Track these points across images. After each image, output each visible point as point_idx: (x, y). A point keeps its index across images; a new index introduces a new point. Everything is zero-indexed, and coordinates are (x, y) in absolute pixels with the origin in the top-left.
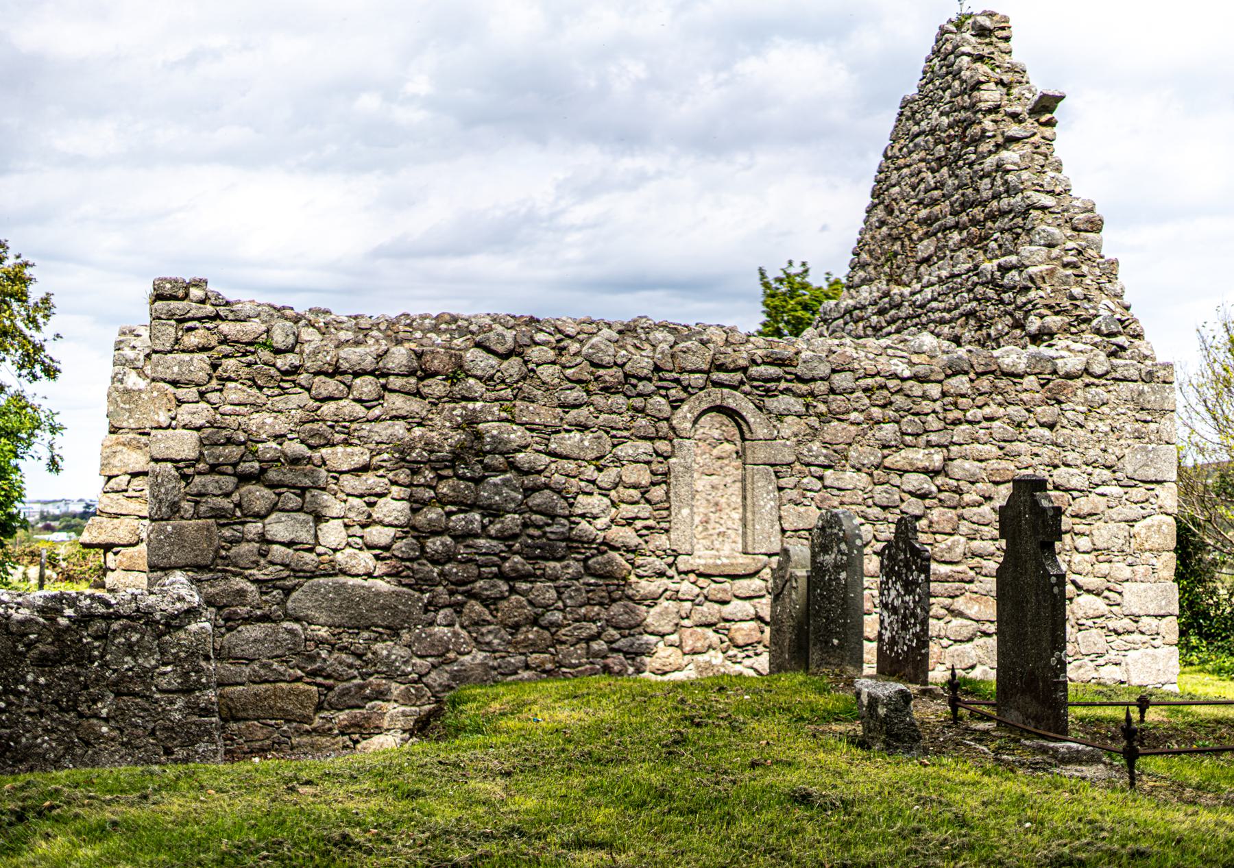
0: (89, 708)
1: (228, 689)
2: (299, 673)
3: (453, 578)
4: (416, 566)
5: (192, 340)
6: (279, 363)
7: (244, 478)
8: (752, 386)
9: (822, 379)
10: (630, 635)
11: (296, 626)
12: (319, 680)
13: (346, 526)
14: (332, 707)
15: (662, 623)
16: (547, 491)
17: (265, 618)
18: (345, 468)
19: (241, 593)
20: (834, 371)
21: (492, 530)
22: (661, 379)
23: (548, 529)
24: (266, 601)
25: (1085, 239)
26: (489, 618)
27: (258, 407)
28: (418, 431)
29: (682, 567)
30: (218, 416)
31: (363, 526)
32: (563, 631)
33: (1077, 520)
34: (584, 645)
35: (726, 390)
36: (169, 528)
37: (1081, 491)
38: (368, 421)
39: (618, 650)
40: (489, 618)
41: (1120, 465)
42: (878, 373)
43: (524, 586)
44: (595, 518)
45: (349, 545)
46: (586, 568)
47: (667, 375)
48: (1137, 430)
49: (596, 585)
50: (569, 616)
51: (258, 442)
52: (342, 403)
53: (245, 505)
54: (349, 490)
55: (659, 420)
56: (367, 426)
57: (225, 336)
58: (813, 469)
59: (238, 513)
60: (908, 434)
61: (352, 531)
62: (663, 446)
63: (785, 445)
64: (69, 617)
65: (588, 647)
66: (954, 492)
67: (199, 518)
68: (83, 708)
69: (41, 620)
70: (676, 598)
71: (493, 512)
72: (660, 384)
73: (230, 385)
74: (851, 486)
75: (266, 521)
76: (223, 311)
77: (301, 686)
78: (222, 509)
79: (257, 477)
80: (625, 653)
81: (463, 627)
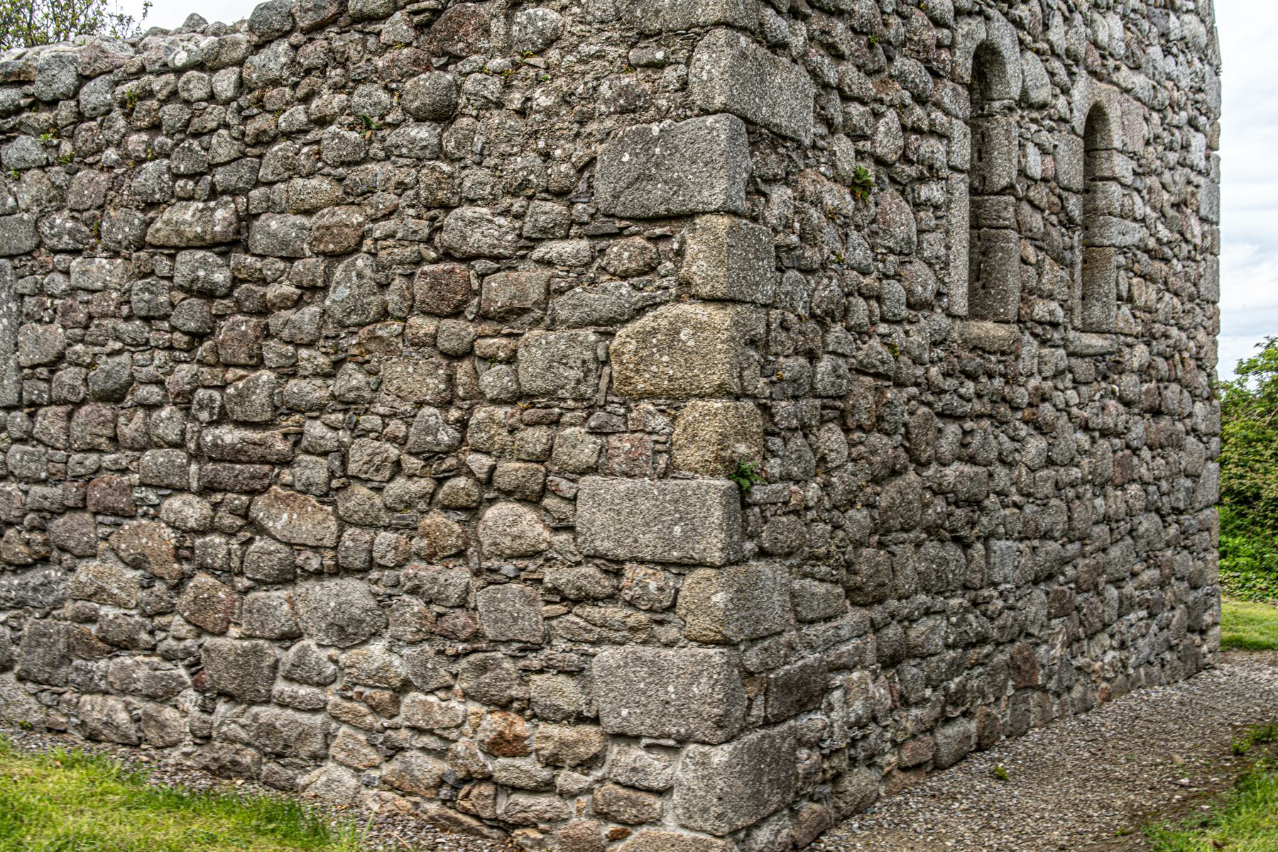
33: (487, 328)
42: (142, 70)
48: (624, 92)
63: (22, 221)
74: (99, 285)
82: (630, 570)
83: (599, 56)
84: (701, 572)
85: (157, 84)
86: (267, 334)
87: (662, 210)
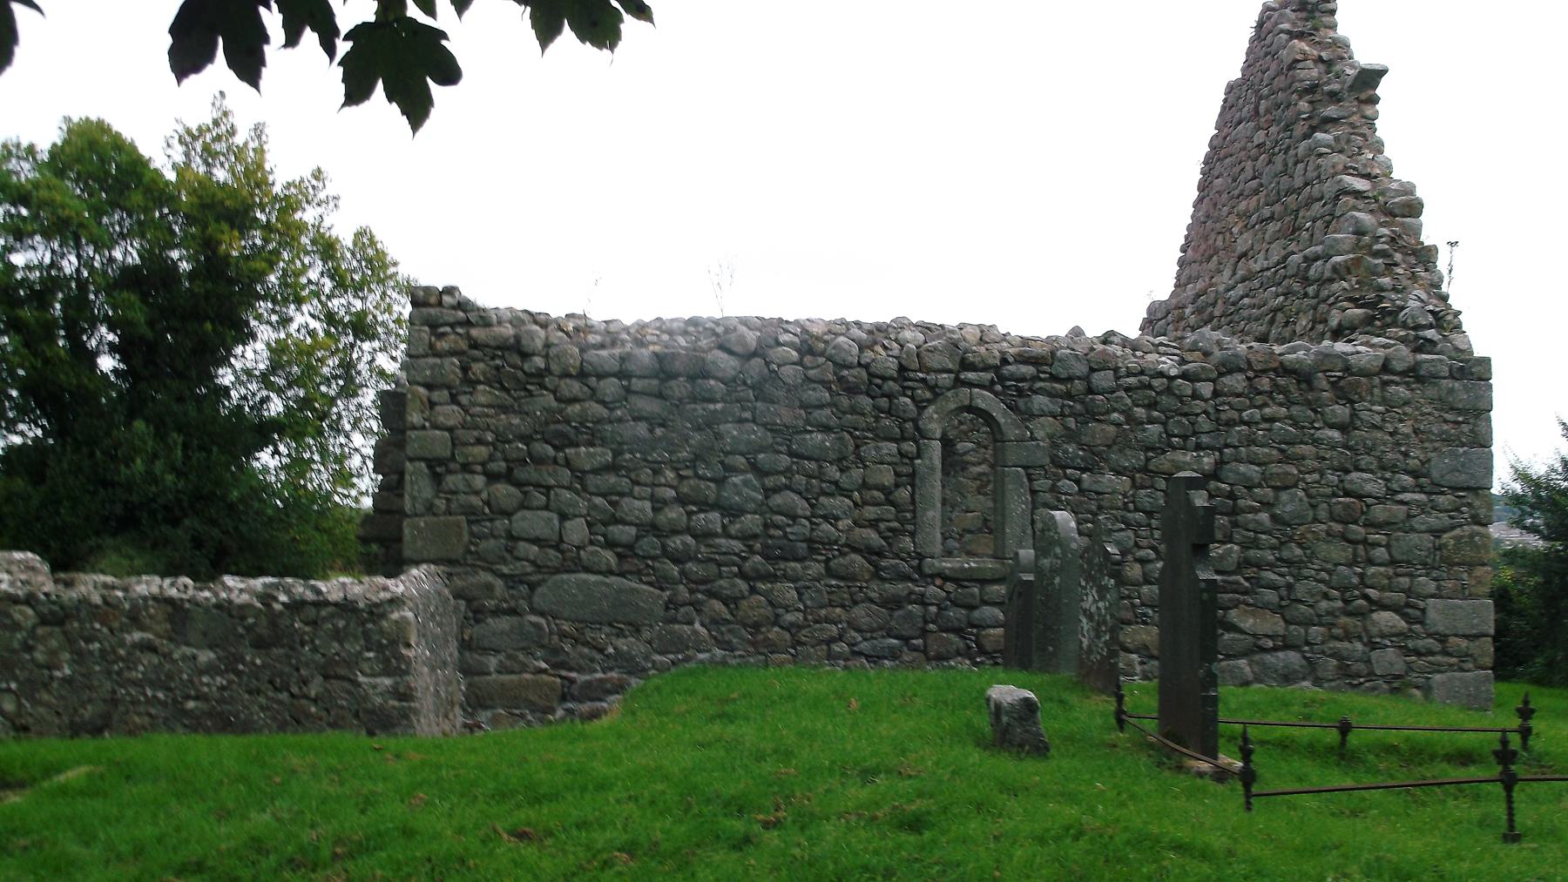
0: (300, 688)
1: (476, 678)
2: (544, 665)
3: (693, 577)
4: (657, 564)
5: (443, 345)
6: (526, 367)
7: (492, 477)
8: (1003, 386)
9: (1079, 378)
10: (872, 638)
11: (542, 621)
12: (564, 673)
13: (589, 525)
14: (574, 699)
15: (906, 626)
16: (788, 492)
17: (513, 612)
18: (587, 468)
19: (489, 587)
20: (1092, 370)
21: (734, 529)
22: (907, 379)
23: (788, 530)
24: (512, 596)
25: (1402, 224)
26: (729, 617)
27: (505, 409)
28: (659, 431)
29: (927, 571)
30: (468, 418)
31: (605, 524)
32: (804, 632)
33: (1373, 531)
34: (825, 647)
35: (976, 390)
36: (422, 524)
37: (1376, 498)
38: (611, 422)
39: (860, 654)
40: (729, 617)
41: (1424, 471)
42: (1142, 372)
43: (761, 586)
44: (837, 519)
45: (591, 543)
46: (828, 569)
47: (912, 375)
48: (1444, 432)
49: (838, 587)
50: (810, 617)
51: (504, 442)
52: (587, 405)
53: (493, 503)
54: (593, 490)
55: (905, 421)
56: (608, 427)
57: (476, 342)
58: (1068, 471)
59: (487, 510)
60: (1176, 436)
61: (595, 529)
62: (909, 447)
64: (283, 604)
65: (829, 648)
66: (1228, 497)
67: (450, 514)
68: (295, 690)
69: (259, 605)
70: (922, 601)
71: (732, 512)
72: (906, 384)
73: (481, 387)
75: (514, 518)
76: (473, 317)
77: (544, 677)
78: (471, 506)
79: (508, 477)
80: (867, 657)
81: (703, 625)
82: (1452, 640)
83: (1429, 414)
84: (1484, 639)
85: (1156, 383)
86: (1235, 524)
87: (1465, 485)
